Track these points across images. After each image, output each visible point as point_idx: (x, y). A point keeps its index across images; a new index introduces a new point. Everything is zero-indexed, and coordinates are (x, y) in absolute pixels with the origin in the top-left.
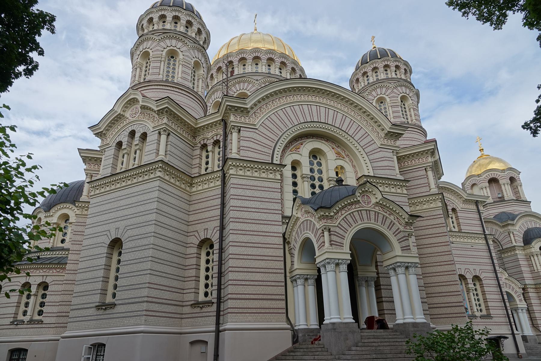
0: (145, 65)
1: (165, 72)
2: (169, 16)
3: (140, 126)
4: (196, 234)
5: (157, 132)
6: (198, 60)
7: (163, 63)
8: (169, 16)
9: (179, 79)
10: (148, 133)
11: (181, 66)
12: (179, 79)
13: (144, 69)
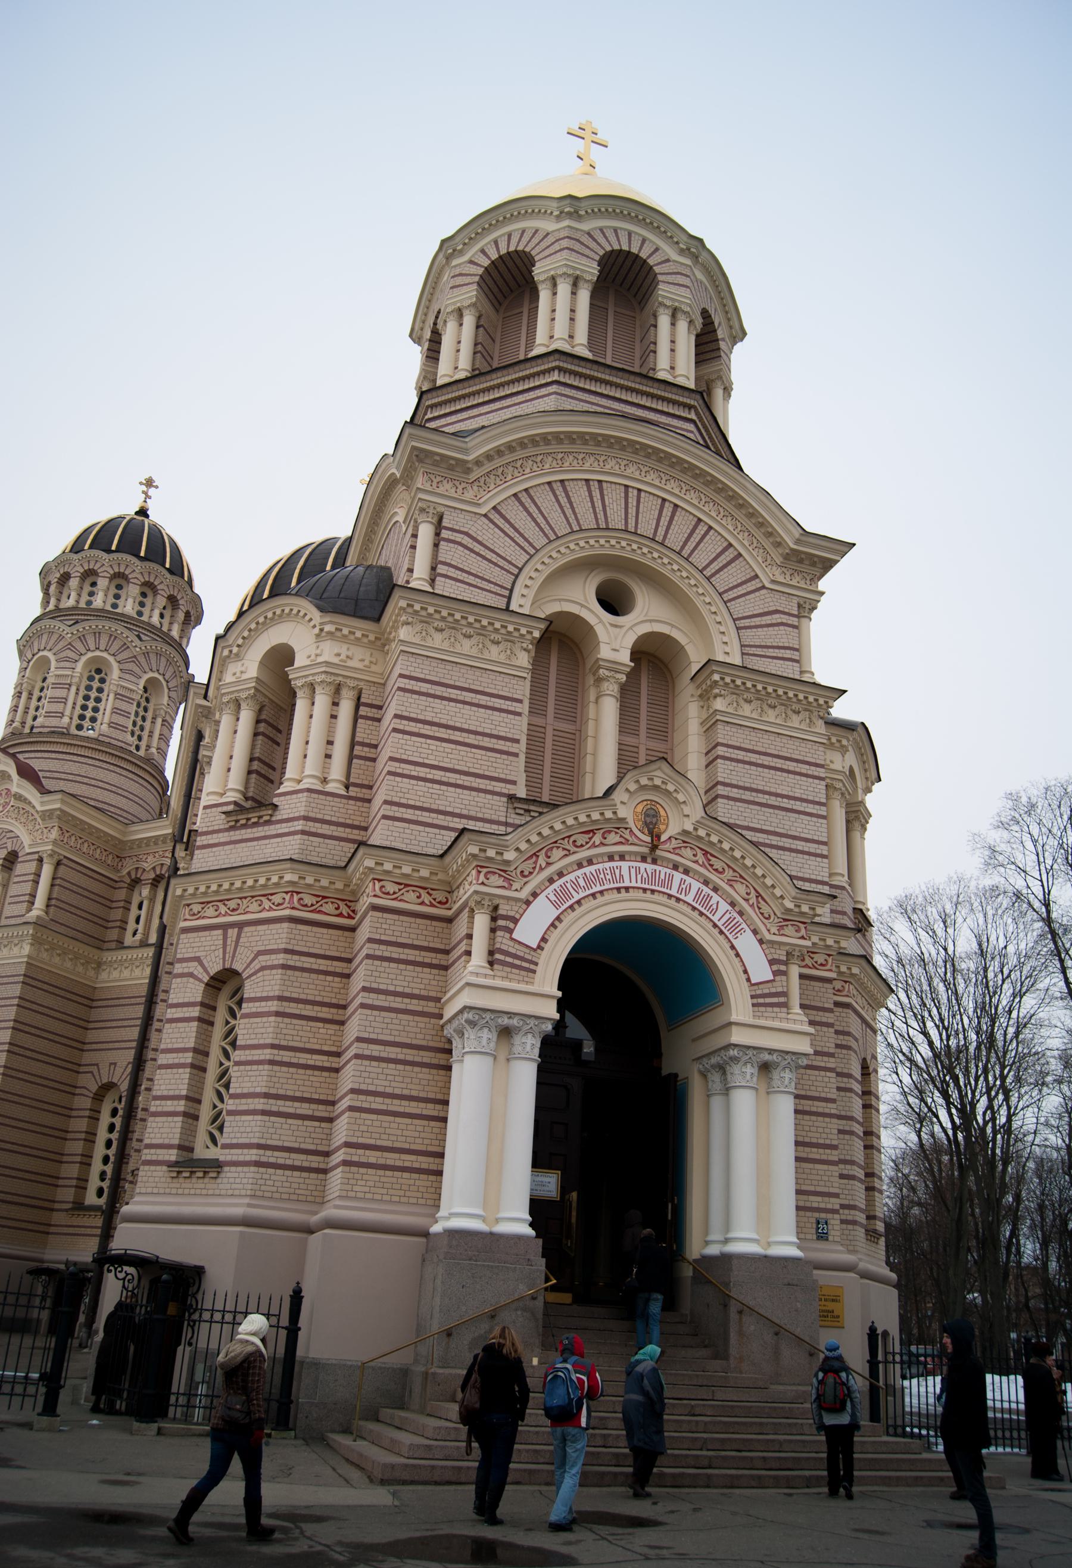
1: (78, 707)
2: (105, 574)
3: (9, 835)
4: (94, 1069)
5: (36, 856)
6: (156, 675)
7: (73, 689)
8: (105, 574)
9: (105, 727)
10: (20, 855)
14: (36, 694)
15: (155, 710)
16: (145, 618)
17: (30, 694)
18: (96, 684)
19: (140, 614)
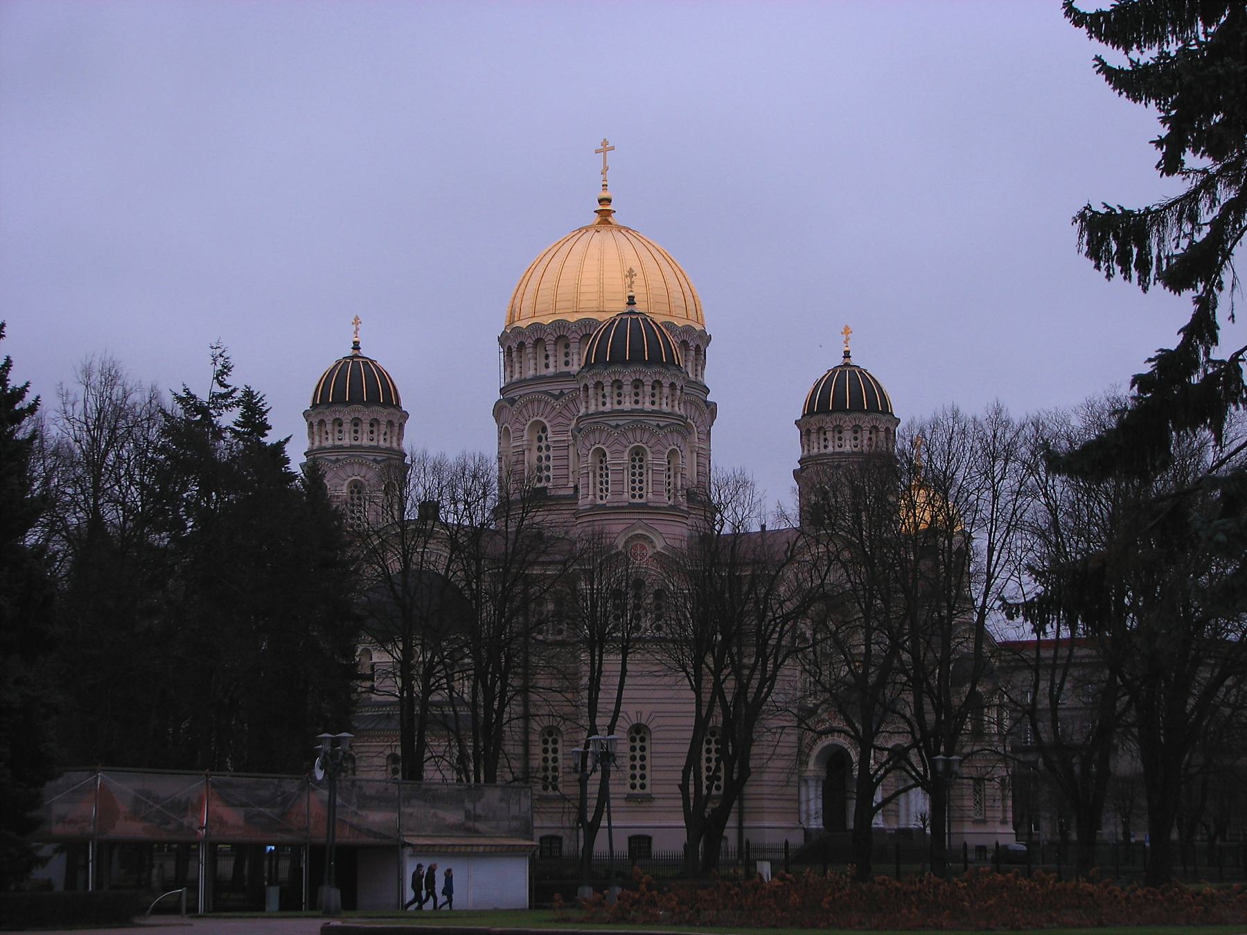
0: (599, 465)
6: (675, 447)
7: (626, 472)
9: (650, 495)
11: (650, 472)
12: (650, 495)
13: (598, 472)
14: (598, 472)
15: (675, 469)
16: (656, 407)
17: (594, 473)
18: (637, 464)
19: (653, 403)
